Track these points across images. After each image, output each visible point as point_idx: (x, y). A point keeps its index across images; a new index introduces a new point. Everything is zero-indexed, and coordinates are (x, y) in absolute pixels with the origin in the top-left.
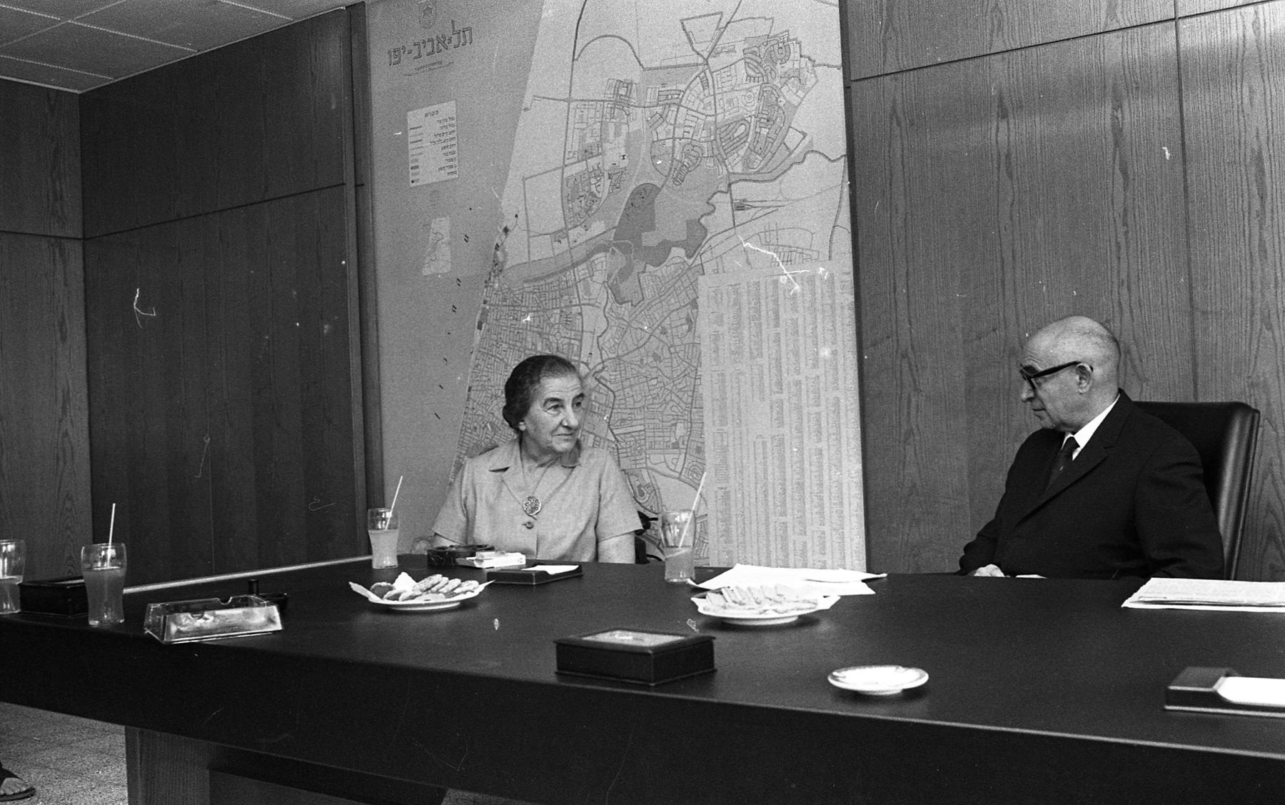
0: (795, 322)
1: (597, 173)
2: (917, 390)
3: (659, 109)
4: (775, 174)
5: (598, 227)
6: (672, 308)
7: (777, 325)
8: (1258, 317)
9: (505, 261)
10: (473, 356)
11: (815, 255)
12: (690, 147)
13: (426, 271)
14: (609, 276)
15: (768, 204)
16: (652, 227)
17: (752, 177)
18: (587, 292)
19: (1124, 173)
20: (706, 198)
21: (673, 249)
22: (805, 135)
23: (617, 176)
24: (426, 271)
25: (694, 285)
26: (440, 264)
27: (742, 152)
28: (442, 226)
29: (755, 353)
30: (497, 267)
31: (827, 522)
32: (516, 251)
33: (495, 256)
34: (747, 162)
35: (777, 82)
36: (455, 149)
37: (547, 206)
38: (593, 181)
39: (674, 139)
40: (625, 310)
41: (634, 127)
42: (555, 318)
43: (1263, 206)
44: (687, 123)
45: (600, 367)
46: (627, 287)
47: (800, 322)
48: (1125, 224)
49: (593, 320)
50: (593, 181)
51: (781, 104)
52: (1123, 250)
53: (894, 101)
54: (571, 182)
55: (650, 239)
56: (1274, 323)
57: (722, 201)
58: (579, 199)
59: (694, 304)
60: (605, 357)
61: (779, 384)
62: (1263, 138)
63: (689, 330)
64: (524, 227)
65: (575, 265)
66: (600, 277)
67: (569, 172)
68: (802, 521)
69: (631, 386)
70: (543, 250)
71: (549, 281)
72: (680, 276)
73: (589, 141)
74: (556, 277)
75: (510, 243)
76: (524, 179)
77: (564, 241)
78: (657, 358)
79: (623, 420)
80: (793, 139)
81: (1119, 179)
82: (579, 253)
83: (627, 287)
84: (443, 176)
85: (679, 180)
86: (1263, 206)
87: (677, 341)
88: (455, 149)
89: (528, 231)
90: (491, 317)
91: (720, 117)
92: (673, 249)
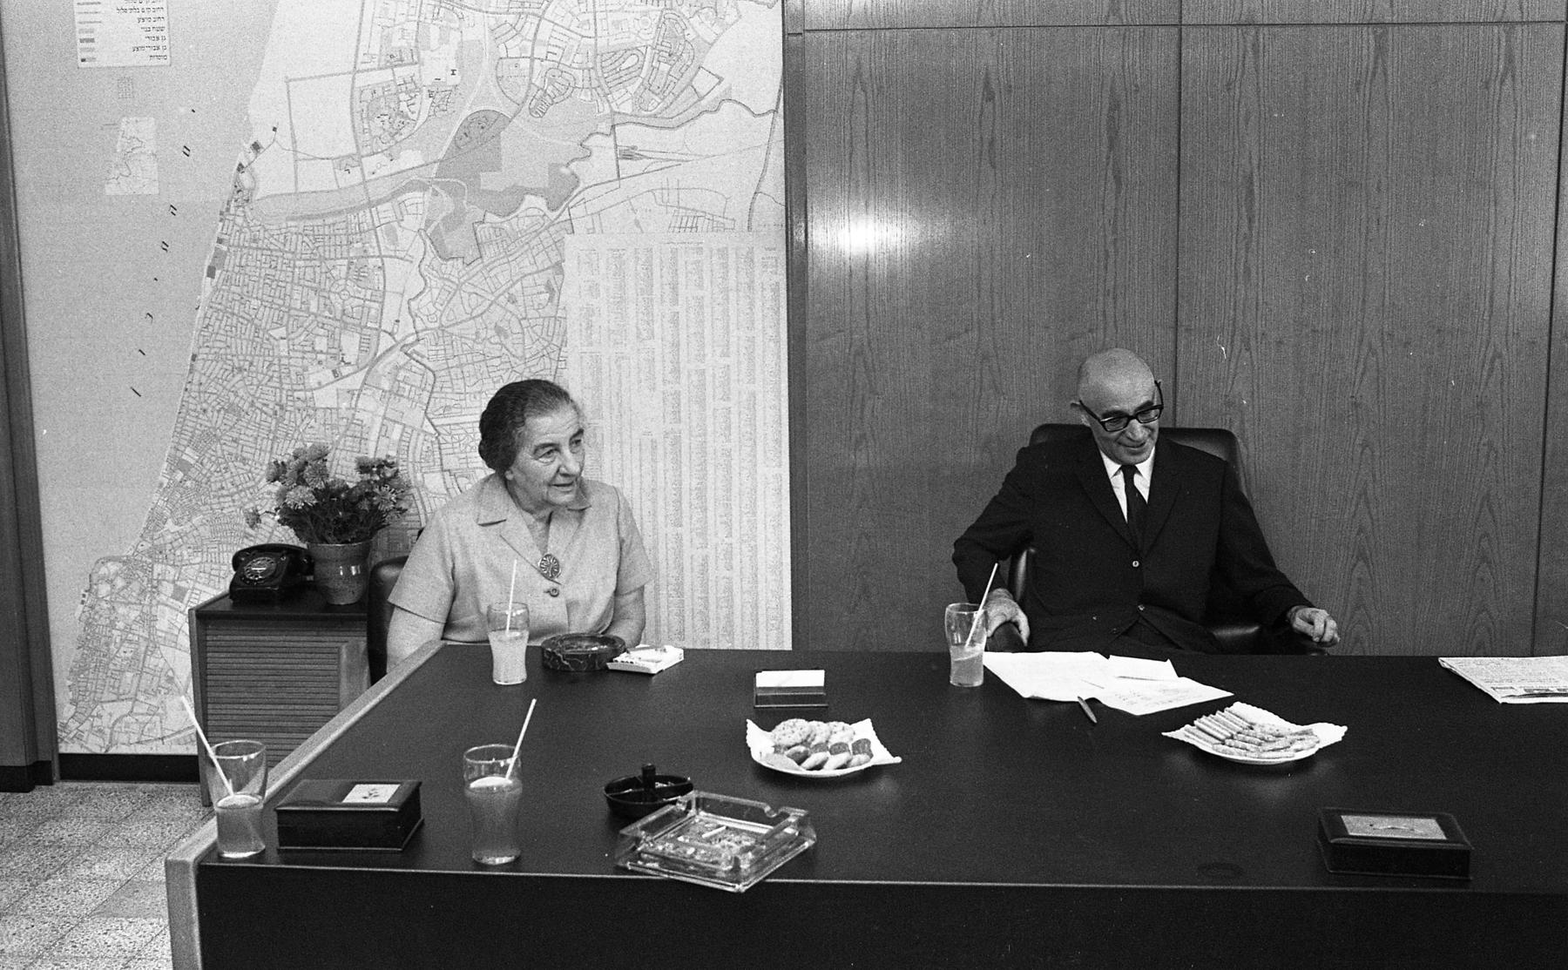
0: (700, 300)
1: (411, 88)
2: (873, 392)
3: (511, 19)
4: (674, 122)
5: (410, 158)
6: (527, 271)
7: (675, 301)
8: (1238, 337)
9: (251, 190)
10: (200, 313)
11: (729, 224)
12: (557, 73)
13: (111, 189)
14: (428, 222)
15: (670, 156)
16: (496, 167)
17: (645, 121)
18: (395, 241)
19: (1118, 179)
20: (579, 139)
21: (528, 197)
22: (721, 80)
23: (441, 97)
24: (111, 189)
25: (558, 244)
26: (140, 180)
27: (632, 88)
28: (140, 129)
29: (645, 334)
30: (241, 195)
31: (736, 534)
32: (271, 175)
33: (237, 180)
34: (639, 101)
35: (684, 9)
36: (163, 23)
37: (328, 124)
38: (403, 97)
39: (532, 59)
40: (453, 269)
41: (469, 35)
42: (341, 269)
43: (1250, 229)
44: (553, 42)
45: (411, 339)
46: (453, 241)
47: (707, 301)
48: (1114, 232)
49: (401, 277)
50: (403, 97)
51: (689, 38)
52: (1111, 261)
53: (859, 64)
54: (367, 95)
55: (489, 181)
56: (1253, 343)
57: (603, 149)
58: (380, 115)
59: (558, 267)
60: (420, 326)
61: (676, 370)
62: (1255, 162)
63: (550, 299)
64: (289, 145)
65: (370, 205)
66: (412, 222)
67: (361, 80)
68: (703, 533)
69: (461, 366)
70: (319, 177)
71: (330, 220)
72: (538, 233)
73: (397, 43)
74: (343, 218)
75: (261, 164)
76: (288, 81)
77: (356, 172)
78: (499, 331)
79: (447, 408)
80: (703, 82)
81: (1112, 185)
82: (384, 190)
83: (456, 240)
84: (142, 59)
85: (538, 112)
86: (1250, 229)
87: (532, 313)
88: (163, 23)
89: (295, 151)
90: (231, 262)
91: (602, 42)
92: (528, 197)
